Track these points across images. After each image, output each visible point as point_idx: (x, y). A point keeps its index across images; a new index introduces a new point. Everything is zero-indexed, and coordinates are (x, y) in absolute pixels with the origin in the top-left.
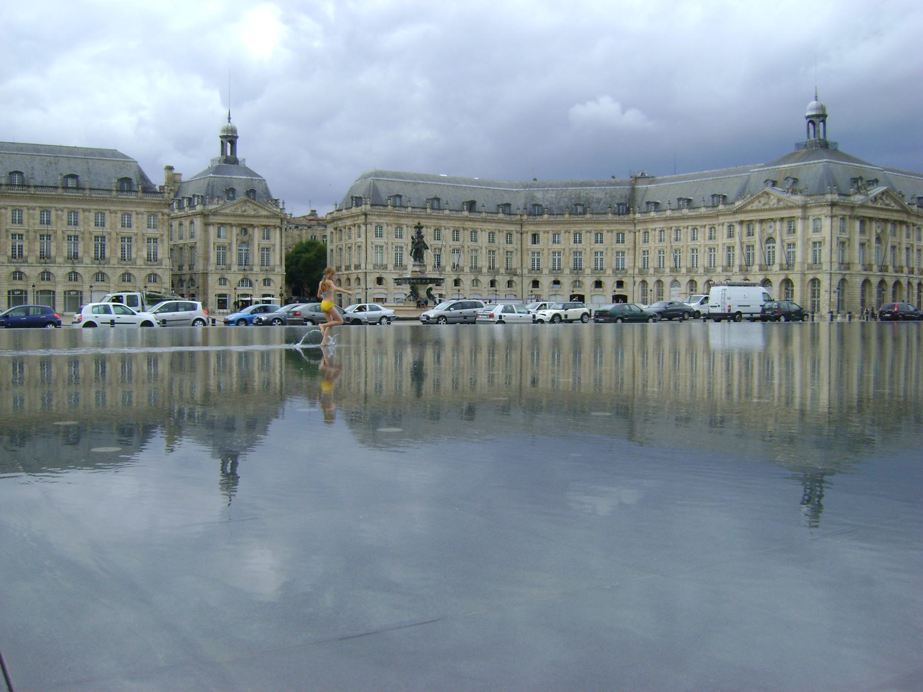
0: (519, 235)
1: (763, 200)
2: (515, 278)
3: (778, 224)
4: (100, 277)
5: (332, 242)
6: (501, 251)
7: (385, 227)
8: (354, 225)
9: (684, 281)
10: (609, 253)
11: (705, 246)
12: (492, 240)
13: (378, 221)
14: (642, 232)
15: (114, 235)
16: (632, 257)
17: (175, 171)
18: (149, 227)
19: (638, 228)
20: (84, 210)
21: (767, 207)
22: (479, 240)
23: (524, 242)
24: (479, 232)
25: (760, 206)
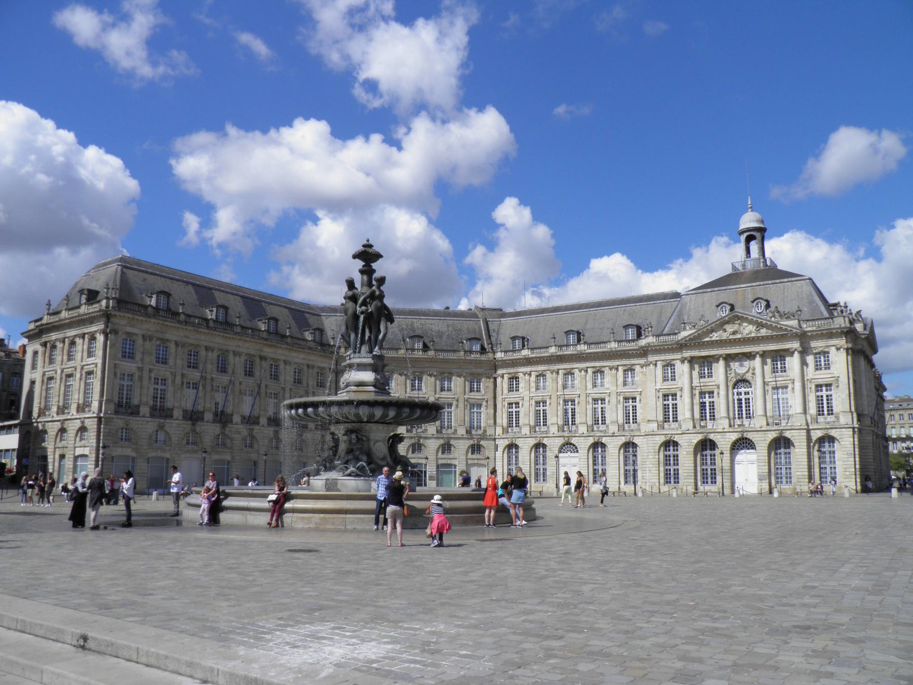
1: (730, 328)
3: (758, 360)
5: (34, 367)
7: (140, 341)
8: (83, 336)
10: (461, 405)
11: (618, 394)
13: (129, 329)
19: (500, 372)
21: (739, 336)
22: (282, 378)
24: (282, 366)
25: (725, 336)
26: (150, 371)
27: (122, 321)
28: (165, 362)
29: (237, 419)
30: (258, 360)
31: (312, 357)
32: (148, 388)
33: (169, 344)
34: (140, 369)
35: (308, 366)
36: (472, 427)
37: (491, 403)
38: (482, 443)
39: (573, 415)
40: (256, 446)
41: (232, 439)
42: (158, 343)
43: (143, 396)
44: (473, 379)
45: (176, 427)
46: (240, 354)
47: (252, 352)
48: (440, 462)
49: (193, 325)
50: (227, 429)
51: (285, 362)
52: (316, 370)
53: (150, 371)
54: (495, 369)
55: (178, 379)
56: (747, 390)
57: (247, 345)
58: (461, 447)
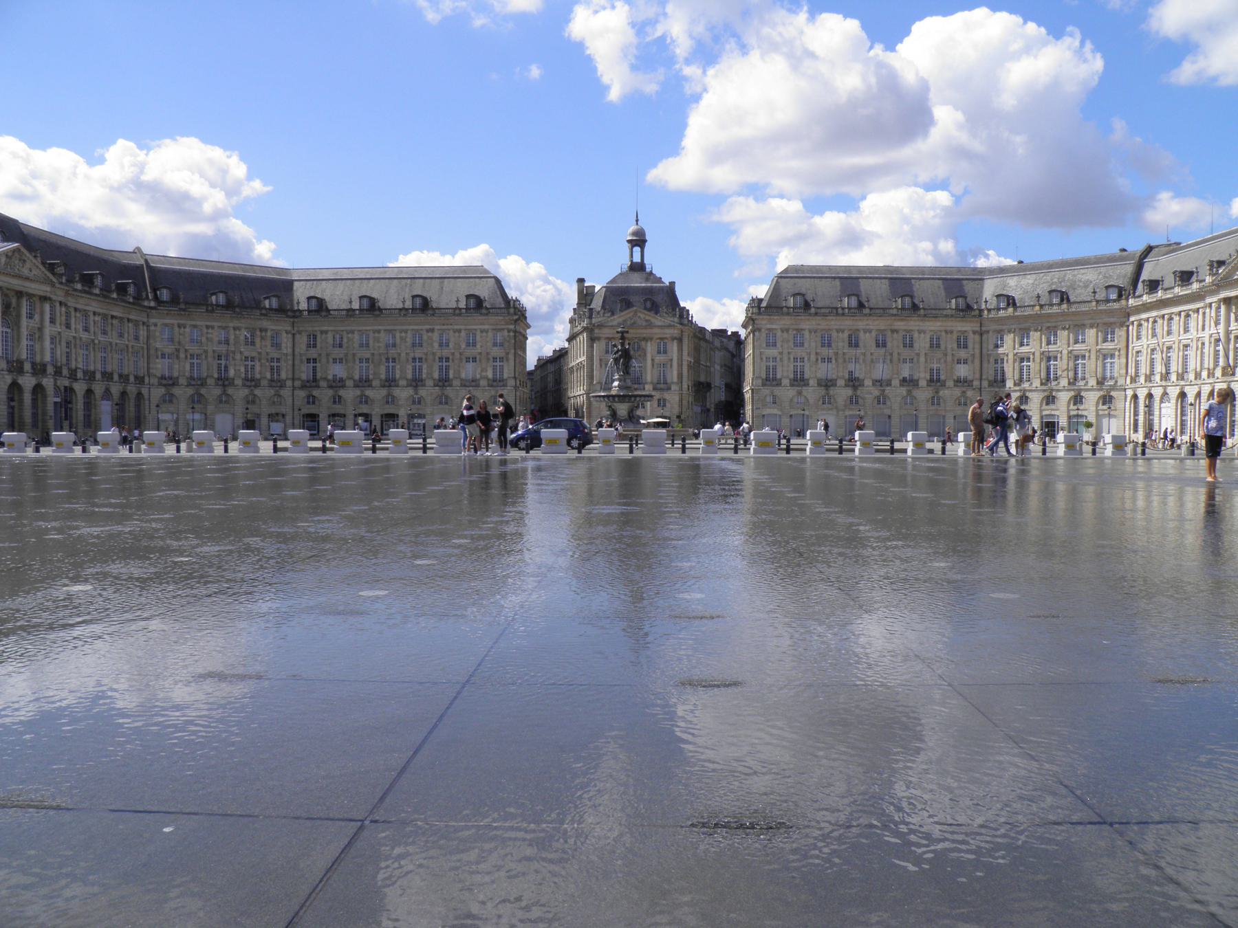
0: (977, 337)
2: (970, 393)
4: (444, 400)
6: (949, 358)
7: (779, 333)
9: (1174, 392)
12: (935, 345)
13: (769, 326)
15: (457, 355)
16: (1124, 360)
17: (586, 284)
18: (495, 344)
19: (1132, 319)
20: (428, 331)
22: (916, 345)
23: (984, 345)
24: (916, 335)
27: (764, 322)
28: (802, 345)
29: (868, 382)
30: (889, 333)
31: (950, 324)
34: (781, 353)
35: (946, 332)
36: (1104, 378)
38: (1113, 393)
40: (888, 403)
41: (863, 399)
43: (785, 371)
44: (1107, 330)
45: (812, 393)
46: (870, 331)
48: (1045, 413)
49: (825, 315)
50: (859, 393)
51: (920, 332)
52: (955, 337)
54: (1128, 315)
55: (813, 357)
58: (1091, 398)
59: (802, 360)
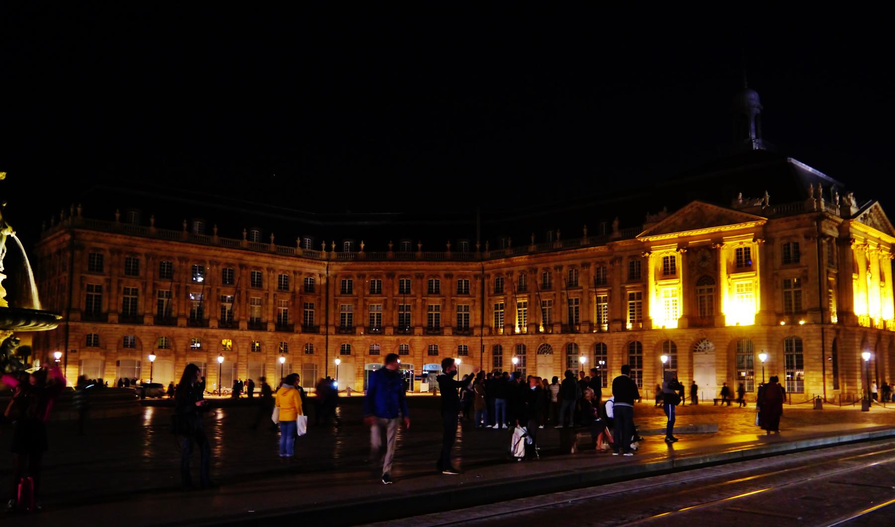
10: (448, 307)
14: (492, 275)
16: (479, 313)
22: (265, 285)
24: (265, 273)
26: (119, 282)
28: (135, 273)
30: (237, 269)
32: (117, 298)
33: (139, 257)
34: (109, 281)
35: (295, 272)
37: (478, 304)
39: (577, 313)
42: (127, 256)
47: (231, 261)
51: (269, 269)
53: (119, 282)
55: (149, 289)
56: (710, 287)
57: (226, 254)
59: (135, 292)
